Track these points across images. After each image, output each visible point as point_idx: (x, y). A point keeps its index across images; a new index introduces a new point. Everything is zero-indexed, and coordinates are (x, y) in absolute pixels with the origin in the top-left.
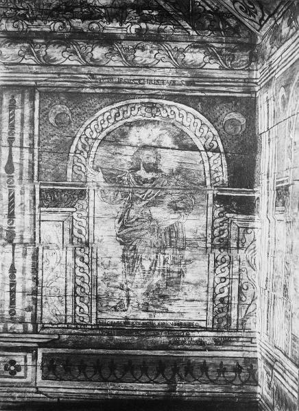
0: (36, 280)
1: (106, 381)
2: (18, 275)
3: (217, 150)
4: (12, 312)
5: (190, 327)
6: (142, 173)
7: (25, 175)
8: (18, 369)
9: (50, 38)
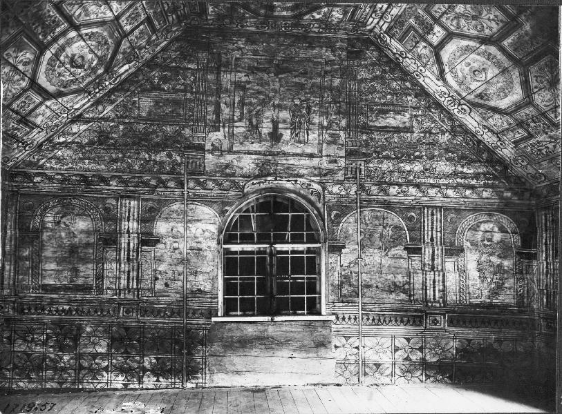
0: (444, 286)
1: (474, 327)
2: (437, 283)
3: (516, 233)
4: (434, 298)
5: (507, 305)
6: (486, 242)
7: (439, 243)
8: (438, 322)
9: (447, 186)
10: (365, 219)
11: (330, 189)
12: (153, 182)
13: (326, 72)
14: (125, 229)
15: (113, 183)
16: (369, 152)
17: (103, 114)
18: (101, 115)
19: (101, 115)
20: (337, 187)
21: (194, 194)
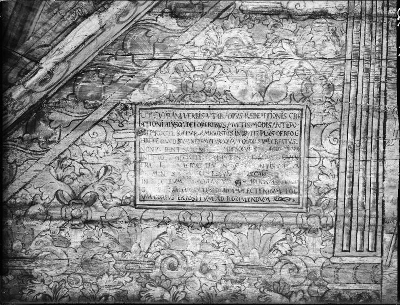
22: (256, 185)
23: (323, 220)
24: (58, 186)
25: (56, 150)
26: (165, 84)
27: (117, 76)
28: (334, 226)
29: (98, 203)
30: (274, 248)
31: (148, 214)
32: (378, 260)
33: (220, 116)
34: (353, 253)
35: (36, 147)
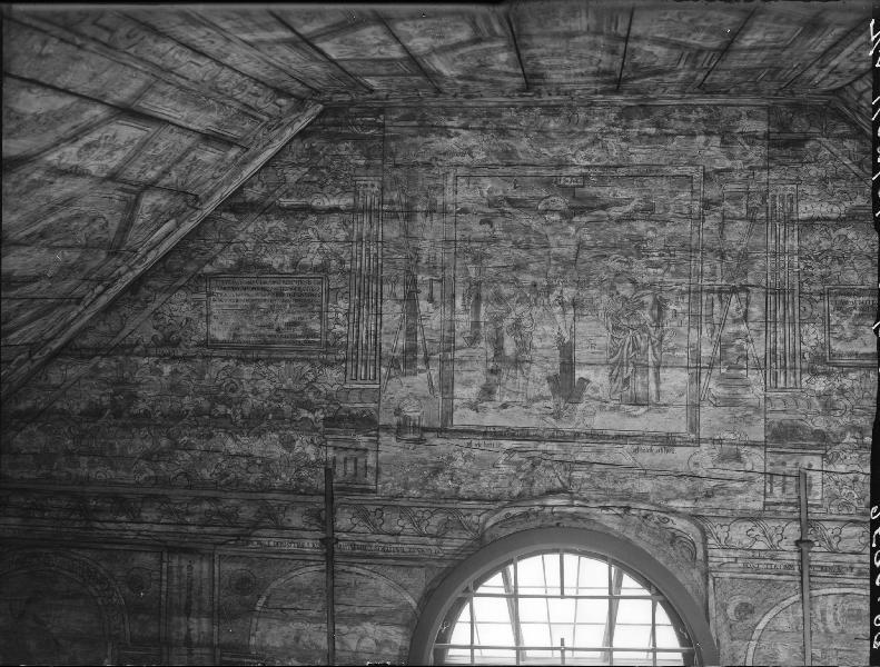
10: (824, 620)
11: (722, 535)
12: (247, 513)
13: (707, 204)
14: (179, 634)
15: (149, 514)
16: (834, 428)
17: (122, 335)
18: (116, 340)
19: (116, 340)
20: (743, 530)
21: (354, 547)
22: (291, 332)
23: (338, 357)
24: (154, 332)
25: (153, 306)
26: (227, 261)
27: (194, 255)
28: (345, 361)
29: (181, 344)
30: (304, 378)
31: (216, 353)
32: (378, 386)
33: (265, 283)
34: (359, 381)
35: (138, 305)
